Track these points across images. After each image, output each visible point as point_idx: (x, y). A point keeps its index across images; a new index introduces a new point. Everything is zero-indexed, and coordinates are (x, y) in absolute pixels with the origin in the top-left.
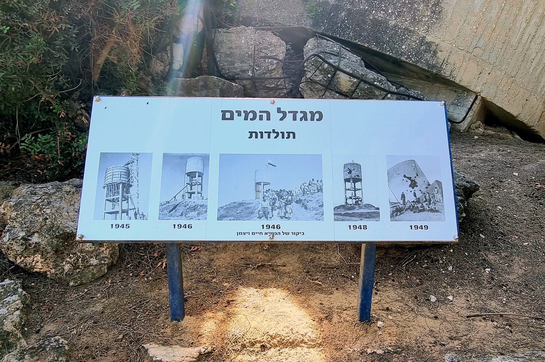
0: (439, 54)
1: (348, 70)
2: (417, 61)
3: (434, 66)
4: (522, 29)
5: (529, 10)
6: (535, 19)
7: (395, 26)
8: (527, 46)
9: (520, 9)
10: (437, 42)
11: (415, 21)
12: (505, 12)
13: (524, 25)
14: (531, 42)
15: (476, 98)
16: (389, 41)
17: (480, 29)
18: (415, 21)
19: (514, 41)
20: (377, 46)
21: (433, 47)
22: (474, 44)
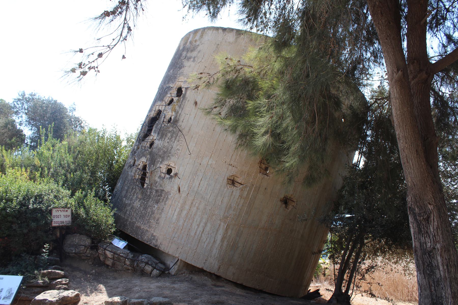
0: (159, 240)
1: (110, 250)
3: (156, 246)
4: (196, 229)
5: (198, 221)
6: (202, 224)
7: (143, 229)
8: (200, 236)
9: (193, 220)
10: (158, 235)
11: (150, 227)
12: (186, 222)
13: (196, 227)
17: (175, 230)
18: (150, 227)
19: (192, 234)
21: (156, 238)
22: (173, 236)
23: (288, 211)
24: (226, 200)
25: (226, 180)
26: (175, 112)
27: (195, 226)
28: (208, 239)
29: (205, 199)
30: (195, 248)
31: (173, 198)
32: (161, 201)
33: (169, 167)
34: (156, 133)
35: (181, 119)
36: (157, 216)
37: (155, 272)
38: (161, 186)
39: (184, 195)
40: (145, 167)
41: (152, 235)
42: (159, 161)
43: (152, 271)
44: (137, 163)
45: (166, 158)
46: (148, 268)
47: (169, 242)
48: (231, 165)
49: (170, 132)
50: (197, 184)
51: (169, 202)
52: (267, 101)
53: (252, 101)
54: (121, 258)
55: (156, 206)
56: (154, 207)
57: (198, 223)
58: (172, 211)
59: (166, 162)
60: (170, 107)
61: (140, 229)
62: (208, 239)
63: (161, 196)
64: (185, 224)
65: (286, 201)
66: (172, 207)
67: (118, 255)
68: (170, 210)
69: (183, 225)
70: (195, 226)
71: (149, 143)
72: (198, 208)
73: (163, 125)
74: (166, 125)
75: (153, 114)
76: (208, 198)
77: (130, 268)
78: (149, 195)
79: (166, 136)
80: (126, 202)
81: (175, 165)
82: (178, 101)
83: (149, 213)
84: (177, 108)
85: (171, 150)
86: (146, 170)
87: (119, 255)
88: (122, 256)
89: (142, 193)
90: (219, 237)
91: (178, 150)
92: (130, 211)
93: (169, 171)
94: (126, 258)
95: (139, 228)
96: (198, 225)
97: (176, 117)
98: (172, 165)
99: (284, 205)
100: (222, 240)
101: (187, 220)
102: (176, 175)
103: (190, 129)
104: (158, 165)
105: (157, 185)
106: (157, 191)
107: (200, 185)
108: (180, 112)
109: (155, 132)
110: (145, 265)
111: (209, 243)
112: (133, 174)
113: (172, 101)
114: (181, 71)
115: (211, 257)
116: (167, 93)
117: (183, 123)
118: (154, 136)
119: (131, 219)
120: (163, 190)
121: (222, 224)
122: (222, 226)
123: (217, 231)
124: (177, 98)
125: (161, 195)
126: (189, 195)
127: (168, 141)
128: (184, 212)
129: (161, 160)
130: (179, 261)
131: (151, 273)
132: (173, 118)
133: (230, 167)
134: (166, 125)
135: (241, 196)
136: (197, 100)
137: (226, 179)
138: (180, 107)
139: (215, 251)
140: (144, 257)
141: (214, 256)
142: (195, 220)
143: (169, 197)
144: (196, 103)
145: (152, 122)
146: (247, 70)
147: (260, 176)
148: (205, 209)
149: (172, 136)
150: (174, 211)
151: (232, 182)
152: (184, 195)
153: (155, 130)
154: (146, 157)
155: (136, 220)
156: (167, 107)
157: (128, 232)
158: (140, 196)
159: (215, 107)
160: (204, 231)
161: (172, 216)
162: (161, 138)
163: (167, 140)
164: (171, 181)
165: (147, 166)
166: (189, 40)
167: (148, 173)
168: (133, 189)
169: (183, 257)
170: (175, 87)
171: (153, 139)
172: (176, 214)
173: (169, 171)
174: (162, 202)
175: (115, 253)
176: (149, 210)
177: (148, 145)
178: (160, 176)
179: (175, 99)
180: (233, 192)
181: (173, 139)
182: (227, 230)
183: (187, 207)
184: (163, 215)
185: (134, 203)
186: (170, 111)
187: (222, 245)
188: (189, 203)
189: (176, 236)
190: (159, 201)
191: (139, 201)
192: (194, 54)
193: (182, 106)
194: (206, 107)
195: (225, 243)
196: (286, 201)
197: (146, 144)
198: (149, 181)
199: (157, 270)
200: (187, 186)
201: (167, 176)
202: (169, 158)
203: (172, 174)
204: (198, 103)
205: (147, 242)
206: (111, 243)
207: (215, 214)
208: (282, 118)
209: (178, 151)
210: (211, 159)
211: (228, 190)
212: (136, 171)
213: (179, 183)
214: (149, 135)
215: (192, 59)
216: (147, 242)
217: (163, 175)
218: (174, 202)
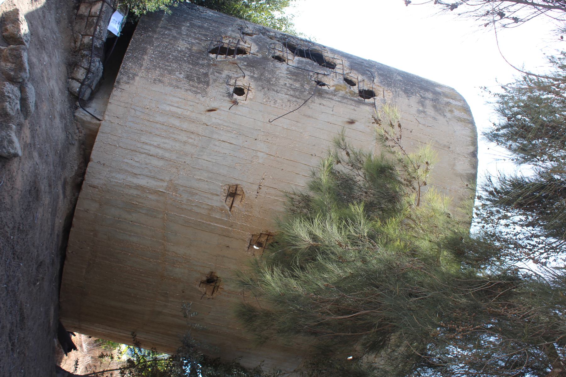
0: (127, 86)
1: (104, 9)
2: (121, 72)
3: (118, 82)
4: (152, 143)
5: (166, 145)
6: (160, 152)
7: (144, 59)
8: (142, 150)
9: (166, 138)
10: (136, 84)
11: (148, 70)
12: (161, 126)
13: (155, 144)
14: (145, 153)
15: (100, 120)
16: (133, 56)
17: (147, 110)
18: (148, 70)
20: (130, 49)
21: (131, 82)
23: (197, 287)
24: (203, 186)
25: (234, 182)
26: (335, 91)
27: (157, 141)
28: (138, 165)
29: (201, 153)
30: (121, 144)
31: (197, 101)
32: (191, 83)
33: (246, 91)
34: (298, 63)
35: (324, 102)
36: (166, 80)
37: (76, 86)
38: (215, 81)
39: (204, 118)
40: (242, 51)
41: (135, 75)
42: (254, 73)
43: (78, 80)
44: (247, 38)
45: (260, 83)
46: (81, 74)
47: (127, 103)
48: (260, 188)
49: (302, 86)
50: (223, 138)
51: (190, 96)
52: (366, 234)
53: (364, 210)
54: (92, 29)
55: (182, 76)
56: (180, 73)
57: (162, 145)
58: (177, 102)
59: (253, 85)
60: (342, 82)
61: (143, 55)
62: (138, 165)
63: (199, 83)
64: (158, 126)
65: (211, 280)
66: (184, 101)
67: (97, 22)
68: (178, 100)
69: (157, 123)
70: (157, 141)
71: (281, 54)
72: (185, 143)
73: (311, 74)
74: (313, 79)
75: (328, 56)
76: (204, 157)
77: (78, 44)
78: (198, 64)
79: (295, 80)
80: (183, 28)
81: (251, 99)
82: (353, 94)
83: (170, 66)
84: (342, 93)
85: (274, 90)
86: (238, 54)
87: (97, 24)
88: (95, 30)
89: (200, 52)
90: (143, 182)
91: (275, 102)
92: (169, 35)
93: (240, 91)
94: (93, 36)
95: (144, 51)
96: (158, 147)
97: (327, 93)
98: (250, 95)
99: (205, 279)
100: (138, 187)
101: (164, 127)
102: (235, 103)
103: (309, 117)
104: (247, 73)
105: (216, 74)
106: (206, 75)
107: (223, 143)
108: (334, 98)
109: (299, 62)
110: (85, 69)
111: (132, 166)
112: (229, 34)
113: (351, 83)
114: (401, 92)
115: (110, 171)
116: (363, 74)
117: (318, 105)
118: (294, 61)
119: (157, 38)
120: (208, 84)
121: (165, 184)
122: (161, 184)
123: (153, 178)
124: (357, 91)
125: (200, 81)
126: (205, 126)
127: (288, 85)
128: (177, 123)
129: (255, 76)
130: (98, 122)
131: (73, 78)
132: (325, 88)
133: (256, 187)
134: (313, 79)
135: (212, 209)
136: (356, 123)
137: (238, 182)
138: (344, 97)
139: (120, 177)
140: (98, 65)
141: (112, 177)
142: (167, 141)
143: (199, 96)
144: (352, 122)
145: (314, 55)
146: (413, 198)
147: (248, 236)
148: (186, 155)
149: (295, 90)
150: (176, 105)
151: (233, 193)
152: (204, 118)
153: (302, 61)
154: (258, 52)
155: (156, 46)
156: (342, 77)
157: (136, 36)
158: (195, 48)
159: (348, 154)
160: (150, 157)
161: (168, 103)
162: (292, 73)
163: (289, 82)
164: (224, 96)
165: (244, 56)
166: (451, 101)
167: (234, 57)
168: (205, 36)
169: (105, 127)
170: (374, 86)
171: (288, 59)
172: (173, 109)
173: (240, 91)
174: (190, 85)
175: (99, 17)
176: (175, 65)
177: (278, 53)
178: (230, 78)
179: (355, 89)
180: (217, 195)
181: (292, 92)
182: (156, 192)
183: (185, 126)
184: (169, 89)
185: (183, 40)
186: (336, 83)
187: (131, 187)
188: (192, 127)
189: (138, 113)
190: (190, 80)
191: (187, 48)
192: (430, 111)
193: (345, 101)
194: (347, 139)
195: (135, 192)
196: (211, 280)
197: (280, 50)
198: (221, 61)
199: (80, 88)
200: (219, 122)
201: (232, 89)
202: (260, 88)
203: (235, 96)
204: (353, 126)
205: (124, 68)
206: (114, 10)
207: (178, 171)
208: (341, 260)
209: (272, 102)
210: (266, 156)
211: (220, 188)
212: (234, 38)
213: (222, 108)
214: (293, 52)
215: (421, 108)
216: (124, 68)
217: (232, 82)
218: (192, 103)
